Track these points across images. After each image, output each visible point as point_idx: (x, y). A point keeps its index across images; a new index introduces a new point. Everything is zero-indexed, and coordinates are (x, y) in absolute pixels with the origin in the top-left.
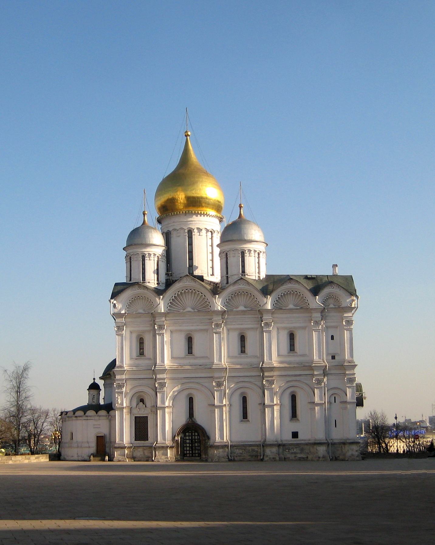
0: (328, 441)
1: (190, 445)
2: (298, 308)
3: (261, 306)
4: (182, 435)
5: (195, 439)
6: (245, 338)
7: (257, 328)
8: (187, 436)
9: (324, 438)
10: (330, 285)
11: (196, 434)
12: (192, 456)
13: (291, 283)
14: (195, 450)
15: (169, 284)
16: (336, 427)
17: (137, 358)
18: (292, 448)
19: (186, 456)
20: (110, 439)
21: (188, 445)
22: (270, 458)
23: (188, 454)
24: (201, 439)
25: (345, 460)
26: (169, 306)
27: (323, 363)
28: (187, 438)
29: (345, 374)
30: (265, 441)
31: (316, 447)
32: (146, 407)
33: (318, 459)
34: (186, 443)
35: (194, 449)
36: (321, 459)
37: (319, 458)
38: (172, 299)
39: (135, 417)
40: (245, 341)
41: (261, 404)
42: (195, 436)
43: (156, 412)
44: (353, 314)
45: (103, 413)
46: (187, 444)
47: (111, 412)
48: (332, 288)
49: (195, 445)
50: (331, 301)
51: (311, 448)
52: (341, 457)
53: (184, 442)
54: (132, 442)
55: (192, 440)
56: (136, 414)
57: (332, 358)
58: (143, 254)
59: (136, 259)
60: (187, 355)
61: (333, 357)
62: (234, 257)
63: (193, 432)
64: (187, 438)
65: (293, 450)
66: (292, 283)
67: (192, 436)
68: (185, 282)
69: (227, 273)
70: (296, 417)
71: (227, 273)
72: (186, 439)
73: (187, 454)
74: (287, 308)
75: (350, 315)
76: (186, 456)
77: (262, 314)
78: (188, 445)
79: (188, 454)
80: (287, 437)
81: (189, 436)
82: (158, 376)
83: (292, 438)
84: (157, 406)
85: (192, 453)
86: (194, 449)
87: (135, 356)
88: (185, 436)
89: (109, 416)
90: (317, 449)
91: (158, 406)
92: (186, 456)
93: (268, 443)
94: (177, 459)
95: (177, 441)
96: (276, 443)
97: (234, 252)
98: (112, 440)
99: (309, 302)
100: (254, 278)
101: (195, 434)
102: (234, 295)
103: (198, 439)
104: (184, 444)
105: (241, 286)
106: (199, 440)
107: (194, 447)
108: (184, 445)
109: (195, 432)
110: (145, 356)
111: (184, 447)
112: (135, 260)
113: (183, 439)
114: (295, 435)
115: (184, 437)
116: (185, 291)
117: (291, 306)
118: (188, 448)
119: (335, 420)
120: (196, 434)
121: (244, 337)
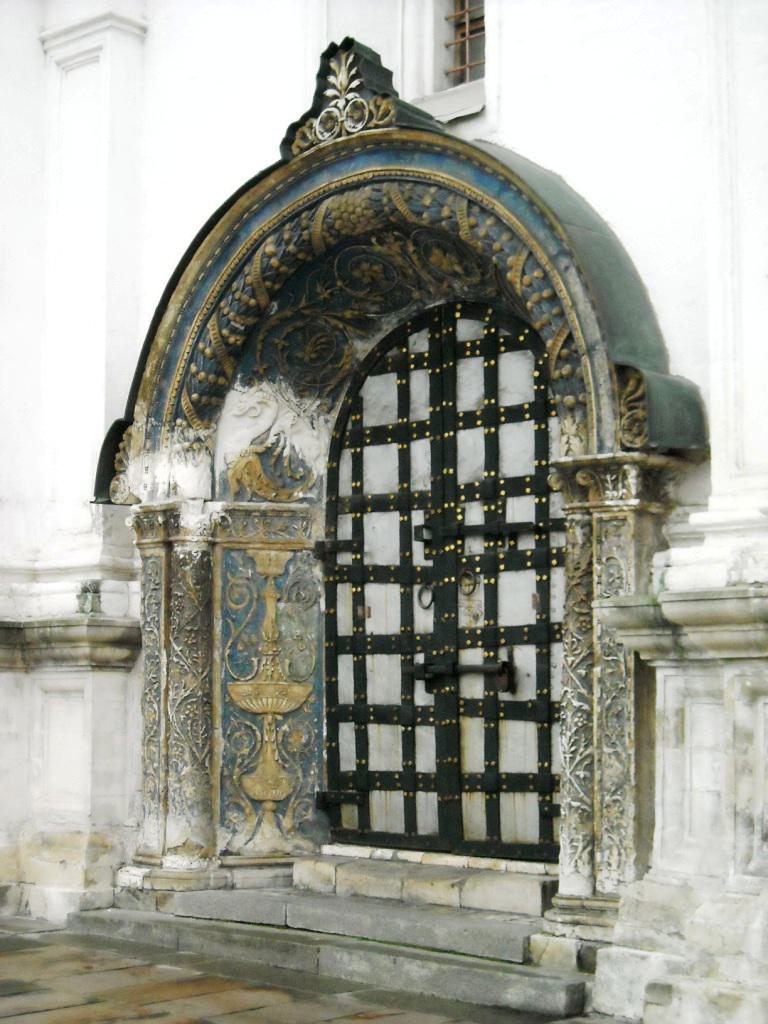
1: (424, 621)
5: (493, 490)
8: (380, 436)
11: (517, 377)
12: (450, 837)
14: (493, 713)
21: (384, 608)
23: (387, 781)
28: (380, 468)
35: (473, 688)
53: (326, 553)
63: (458, 351)
67: (446, 422)
73: (366, 782)
78: (384, 608)
79: (387, 781)
81: (402, 434)
85: (450, 780)
86: (473, 688)
88: (350, 437)
92: (364, 836)
107: (473, 656)
115: (335, 454)
118: (385, 678)
120: (517, 377)
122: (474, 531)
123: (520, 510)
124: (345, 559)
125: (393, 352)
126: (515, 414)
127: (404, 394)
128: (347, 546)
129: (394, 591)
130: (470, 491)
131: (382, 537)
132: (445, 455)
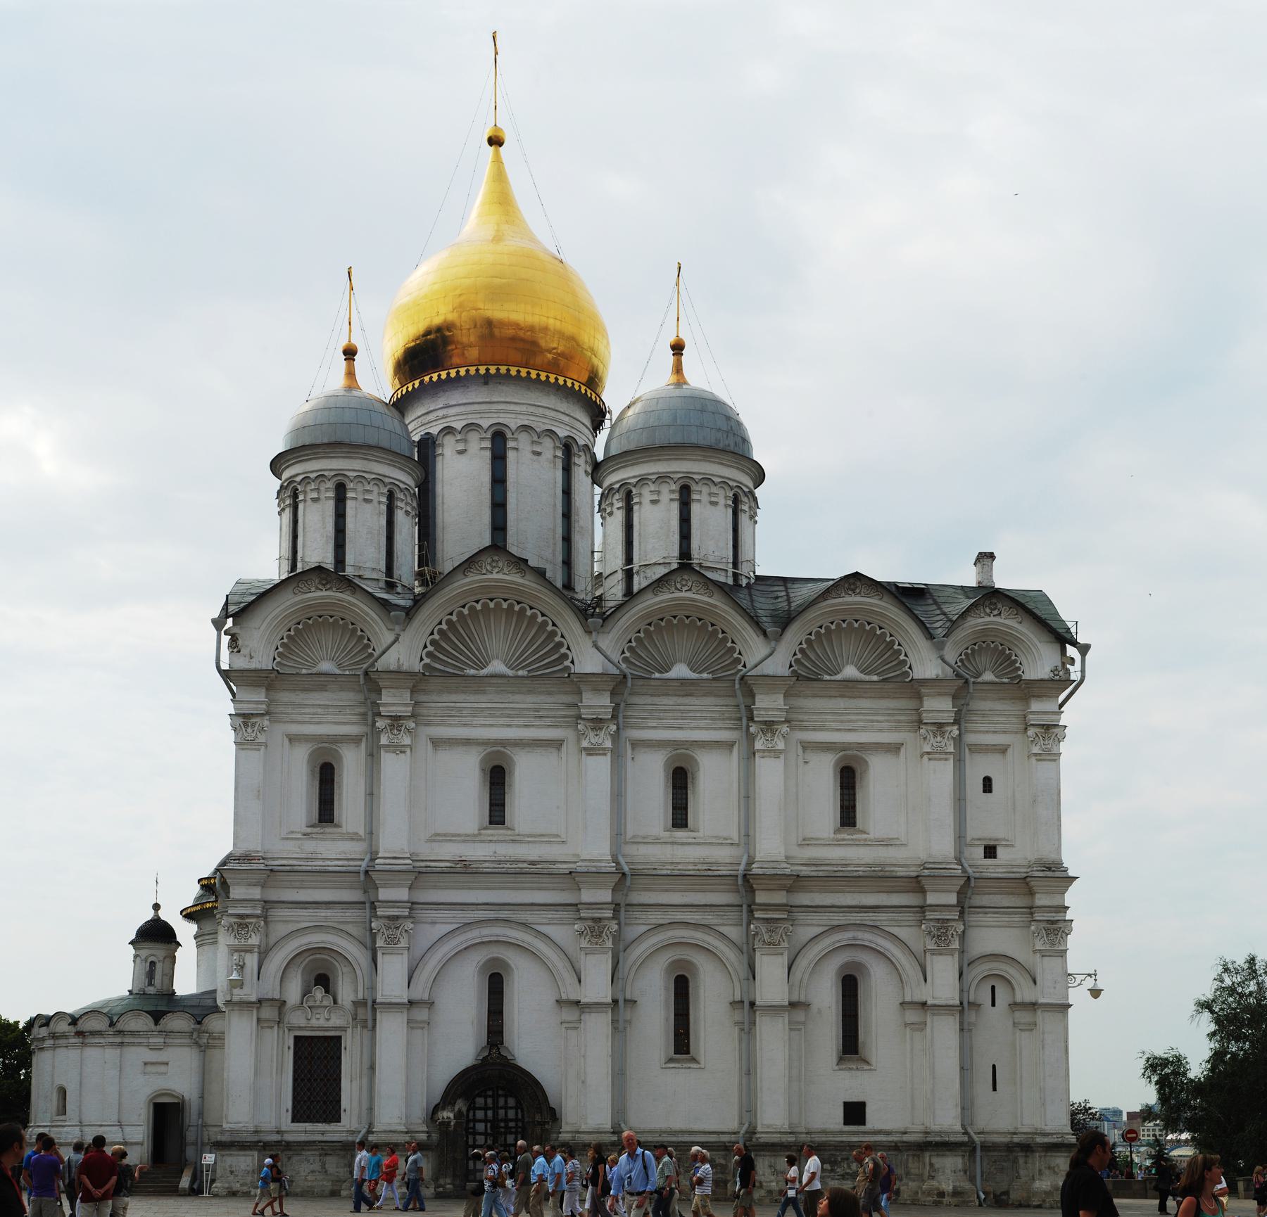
0: (970, 1137)
2: (875, 678)
3: (748, 666)
4: (460, 1105)
5: (506, 1120)
6: (689, 775)
7: (730, 745)
8: (480, 1109)
9: (958, 1128)
10: (987, 603)
13: (853, 590)
15: (431, 578)
16: (995, 1089)
17: (309, 830)
18: (843, 1160)
19: (475, 1177)
20: (201, 1114)
22: (770, 1192)
24: (526, 1120)
25: (1028, 1206)
26: (429, 655)
27: (956, 867)
28: (480, 1114)
29: (1031, 909)
30: (752, 1132)
31: (930, 1156)
32: (335, 1002)
33: (935, 1198)
34: (475, 1133)
36: (946, 1200)
37: (942, 1194)
38: (441, 632)
39: (297, 1039)
40: (686, 788)
41: (742, 1002)
42: (506, 1108)
43: (370, 1024)
44: (1061, 706)
45: (178, 1022)
46: (477, 1137)
47: (213, 1023)
48: (996, 612)
49: (505, 1139)
50: (983, 661)
51: (910, 1160)
52: (1014, 1196)
53: (467, 1129)
54: (284, 1128)
55: (495, 1122)
56: (300, 1028)
57: (985, 853)
58: (339, 478)
59: (315, 495)
60: (485, 829)
61: (990, 852)
62: (654, 502)
63: (499, 1096)
64: (480, 1114)
65: (849, 1167)
66: (858, 591)
67: (495, 1108)
68: (487, 570)
69: (629, 560)
70: (856, 1052)
71: (629, 560)
72: (475, 1121)
74: (838, 677)
75: (1050, 706)
76: (471, 1177)
77: (753, 696)
80: (829, 1119)
81: (486, 1109)
82: (384, 894)
83: (845, 1124)
84: (374, 1002)
87: (304, 823)
88: (472, 1107)
89: (200, 1032)
90: (931, 1165)
91: (377, 1001)
93: (764, 1138)
94: (441, 1189)
95: (446, 1124)
96: (791, 1139)
97: (653, 487)
98: (210, 1120)
99: (912, 660)
100: (722, 579)
101: (506, 1102)
102: (657, 626)
103: (516, 1120)
104: (467, 1138)
105: (683, 594)
106: (520, 1124)
108: (467, 1142)
109: (506, 1096)
110: (338, 826)
111: (467, 1146)
112: (315, 500)
113: (464, 1120)
114: (855, 1112)
115: (468, 1111)
116: (485, 606)
117: (850, 671)
119: (994, 1067)
120: (511, 1102)
121: (686, 773)
122: (502, 1127)
123: (512, 1124)
124: (471, 1130)
125: (483, 1094)
126: (511, 1108)
127: (486, 1102)
128: (471, 1128)
129: (483, 1137)
130: (501, 1120)
131: (480, 1127)
132: (495, 1114)
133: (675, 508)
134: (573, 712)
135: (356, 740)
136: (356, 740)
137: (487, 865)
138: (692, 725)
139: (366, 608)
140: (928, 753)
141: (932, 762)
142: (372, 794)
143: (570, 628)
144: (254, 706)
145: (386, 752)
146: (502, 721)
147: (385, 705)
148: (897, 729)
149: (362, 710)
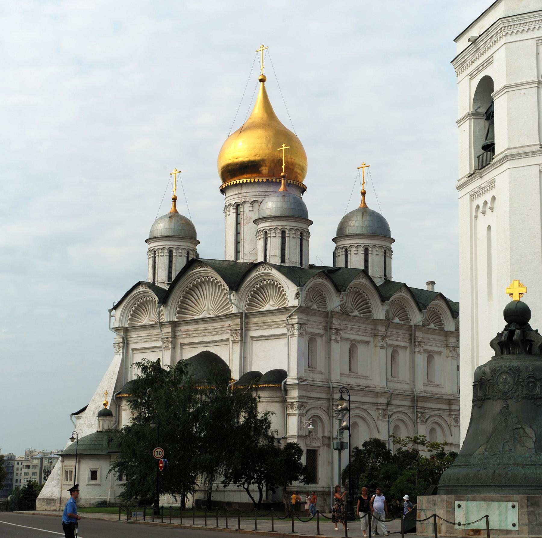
7: (406, 348)
62: (377, 255)
112: (294, 237)
133: (383, 257)
134: (373, 332)
135: (321, 335)
136: (321, 335)
137: (355, 387)
138: (399, 340)
139: (331, 288)
140: (452, 357)
141: (453, 360)
142: (329, 357)
143: (375, 301)
144: (302, 320)
145: (334, 342)
146: (357, 333)
147: (334, 324)
148: (441, 347)
149: (324, 325)
